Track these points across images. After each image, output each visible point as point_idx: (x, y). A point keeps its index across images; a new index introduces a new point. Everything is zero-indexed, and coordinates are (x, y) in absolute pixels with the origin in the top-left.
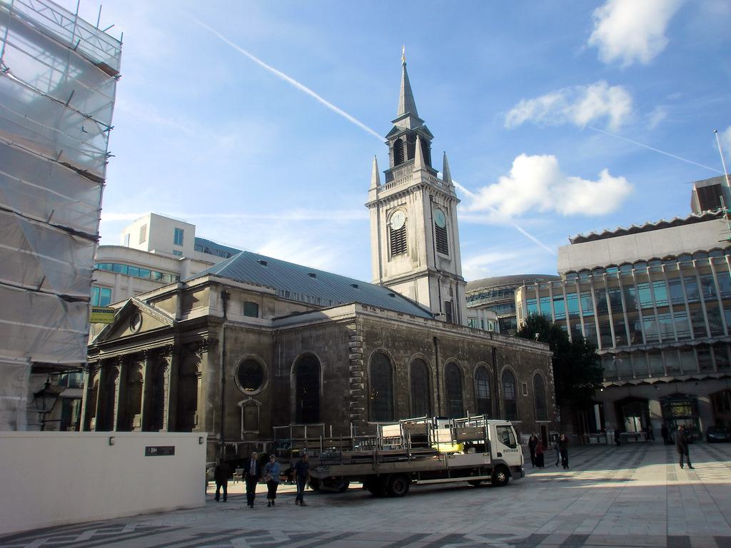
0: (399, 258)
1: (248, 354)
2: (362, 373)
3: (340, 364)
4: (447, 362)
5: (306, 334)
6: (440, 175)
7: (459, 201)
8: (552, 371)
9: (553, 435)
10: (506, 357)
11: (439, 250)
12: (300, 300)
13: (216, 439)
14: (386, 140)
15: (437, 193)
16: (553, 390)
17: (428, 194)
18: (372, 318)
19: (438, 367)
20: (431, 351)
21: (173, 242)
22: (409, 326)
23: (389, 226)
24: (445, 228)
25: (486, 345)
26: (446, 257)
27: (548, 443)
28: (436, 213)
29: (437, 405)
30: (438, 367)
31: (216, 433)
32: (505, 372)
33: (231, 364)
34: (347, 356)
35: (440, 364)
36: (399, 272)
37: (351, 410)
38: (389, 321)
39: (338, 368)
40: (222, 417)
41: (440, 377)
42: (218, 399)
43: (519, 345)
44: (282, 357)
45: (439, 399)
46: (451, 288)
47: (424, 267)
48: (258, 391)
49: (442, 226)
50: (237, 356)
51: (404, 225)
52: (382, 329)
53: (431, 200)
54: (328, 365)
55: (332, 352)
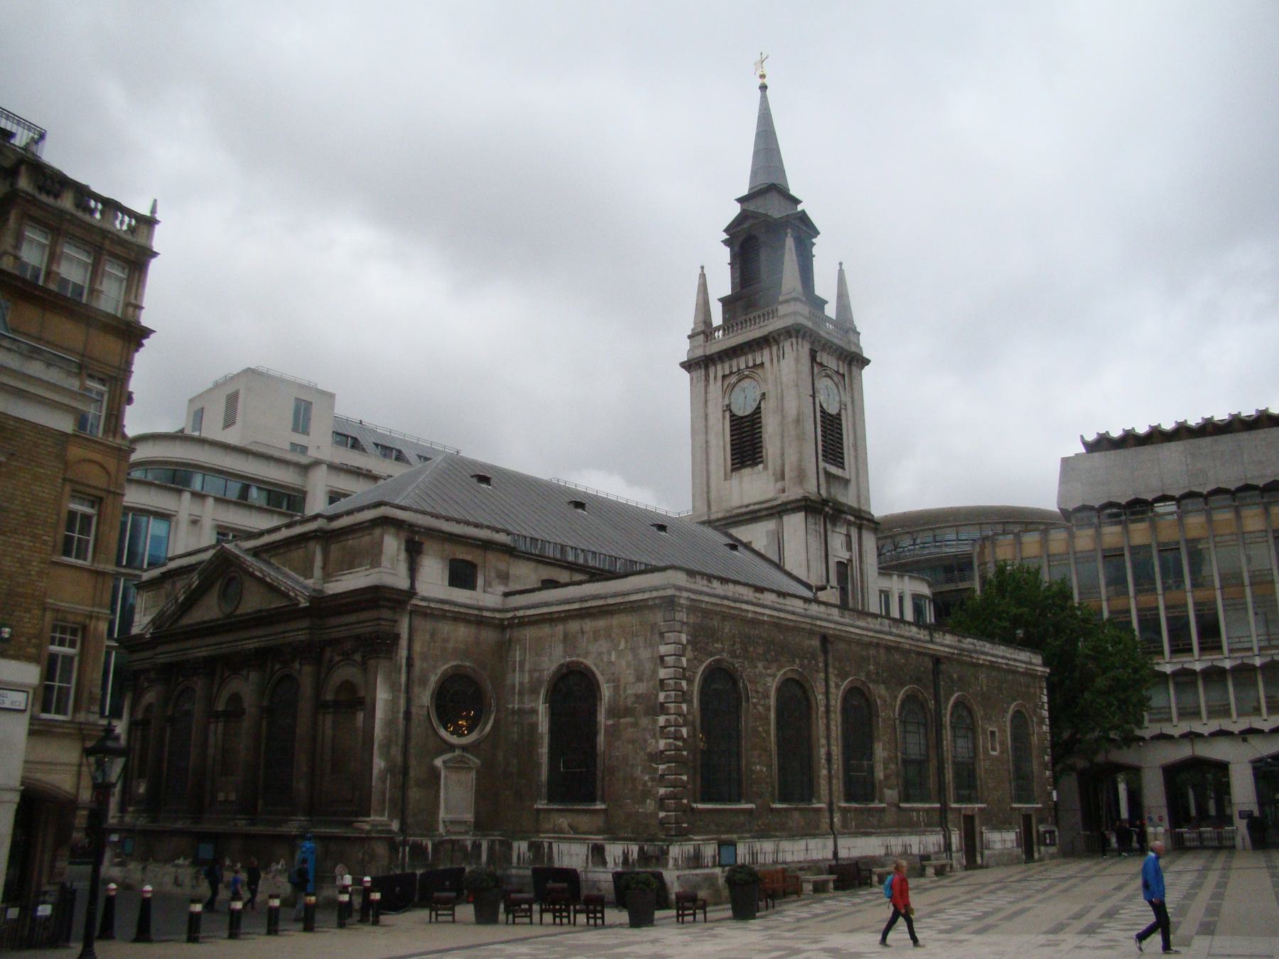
0: (746, 471)
1: (455, 663)
2: (684, 707)
3: (642, 688)
4: (844, 685)
5: (574, 626)
6: (831, 311)
7: (867, 362)
8: (1046, 706)
9: (1046, 832)
10: (960, 679)
11: (826, 458)
12: (558, 556)
13: (390, 832)
14: (726, 236)
16: (1047, 743)
17: (807, 347)
18: (707, 599)
19: (829, 696)
20: (817, 665)
21: (290, 426)
22: (775, 613)
23: (728, 408)
24: (839, 414)
25: (919, 654)
27: (1035, 848)
28: (823, 384)
29: (824, 772)
30: (829, 696)
31: (391, 818)
32: (956, 705)
33: (424, 682)
34: (655, 672)
35: (833, 690)
36: (746, 502)
37: (661, 780)
38: (738, 605)
39: (637, 696)
40: (404, 788)
41: (832, 716)
42: (396, 751)
43: (986, 654)
44: (522, 671)
45: (829, 760)
46: (848, 536)
47: (794, 493)
48: (473, 737)
49: (833, 410)
50: (435, 667)
51: (759, 408)
52: (725, 617)
54: (616, 688)
55: (624, 663)
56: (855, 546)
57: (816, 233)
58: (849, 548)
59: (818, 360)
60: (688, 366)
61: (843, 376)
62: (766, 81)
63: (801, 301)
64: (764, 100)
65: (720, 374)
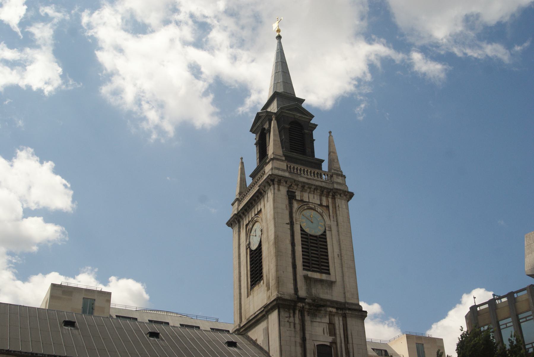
6: (325, 167)
7: (351, 195)
15: (303, 187)
17: (284, 190)
24: (324, 234)
26: (324, 277)
46: (331, 324)
53: (291, 196)
56: (340, 331)
57: (313, 117)
58: (332, 332)
59: (298, 198)
60: (230, 224)
61: (327, 207)
62: (281, 34)
63: (278, 159)
64: (280, 44)
65: (245, 224)
